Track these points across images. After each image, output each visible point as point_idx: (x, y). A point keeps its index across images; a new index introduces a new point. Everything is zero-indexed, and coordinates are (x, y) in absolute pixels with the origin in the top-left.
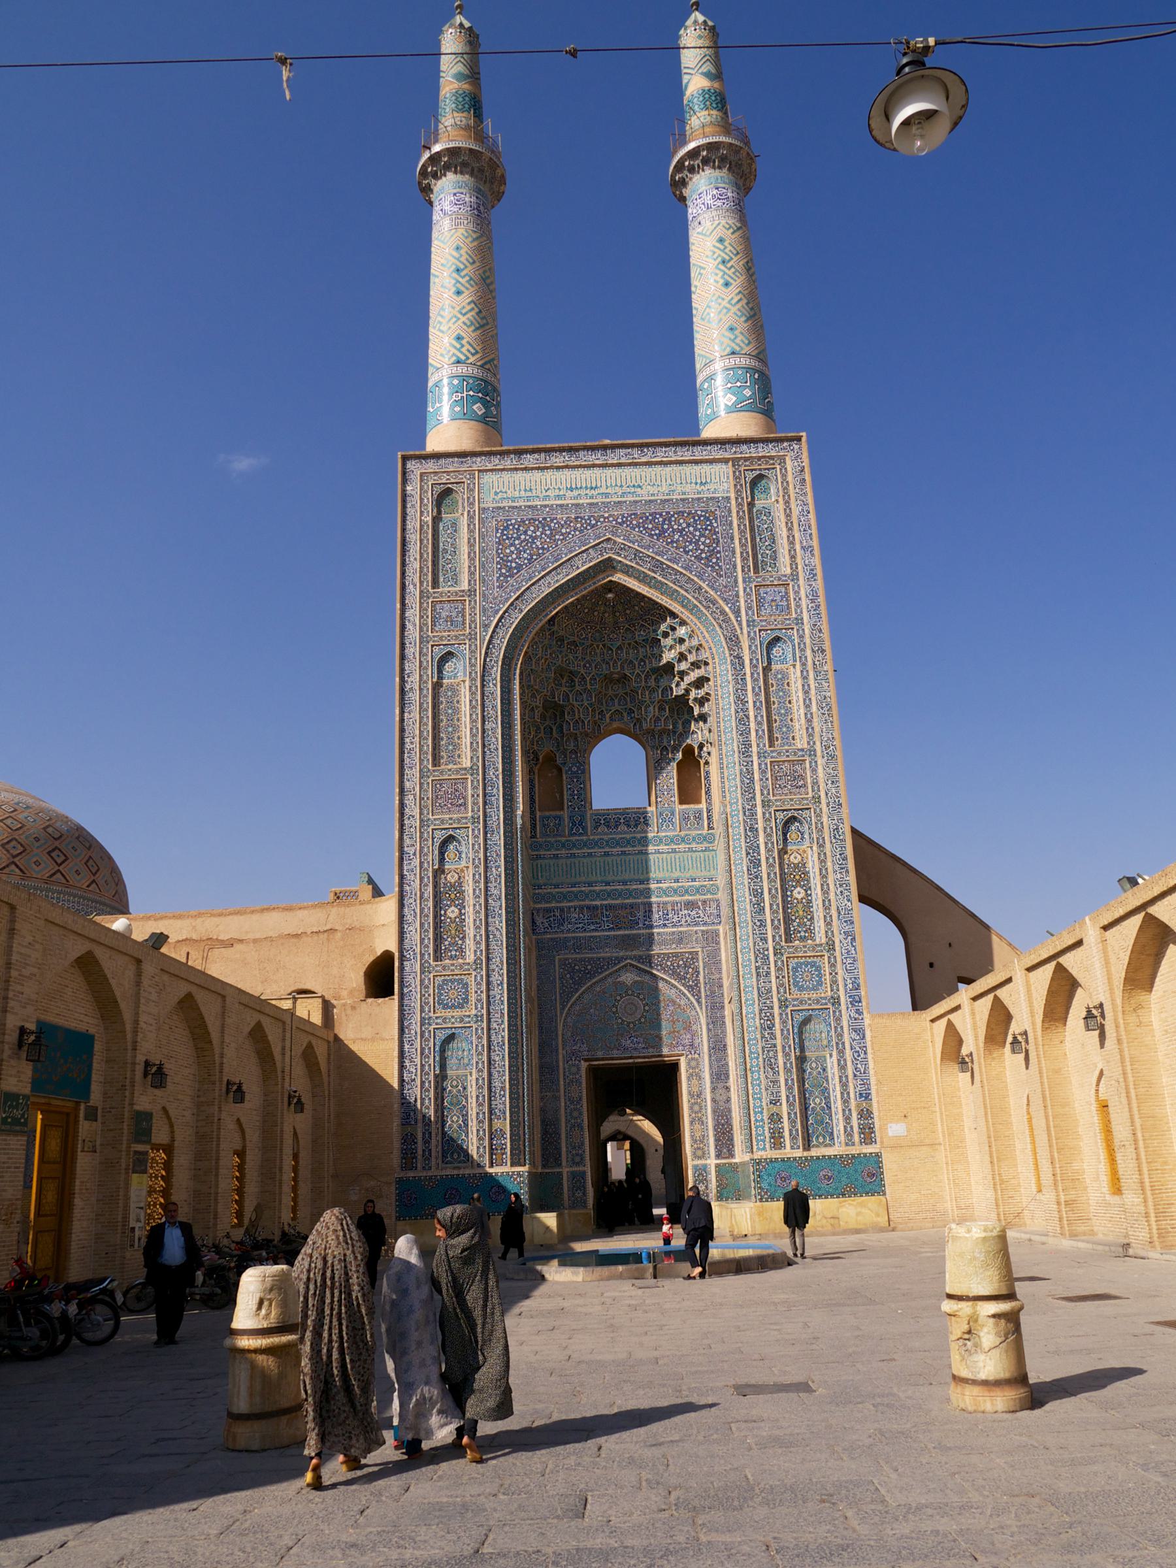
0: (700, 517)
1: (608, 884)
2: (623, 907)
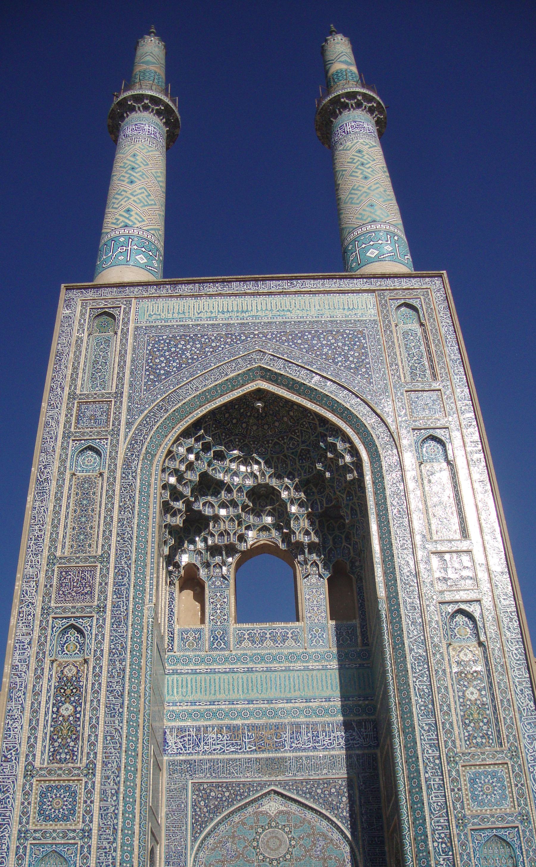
0: (348, 335)
1: (250, 702)
2: (266, 727)
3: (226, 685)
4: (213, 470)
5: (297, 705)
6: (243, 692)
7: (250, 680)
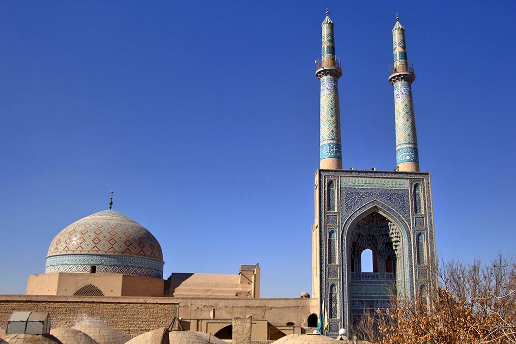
1: (366, 294)
2: (370, 301)
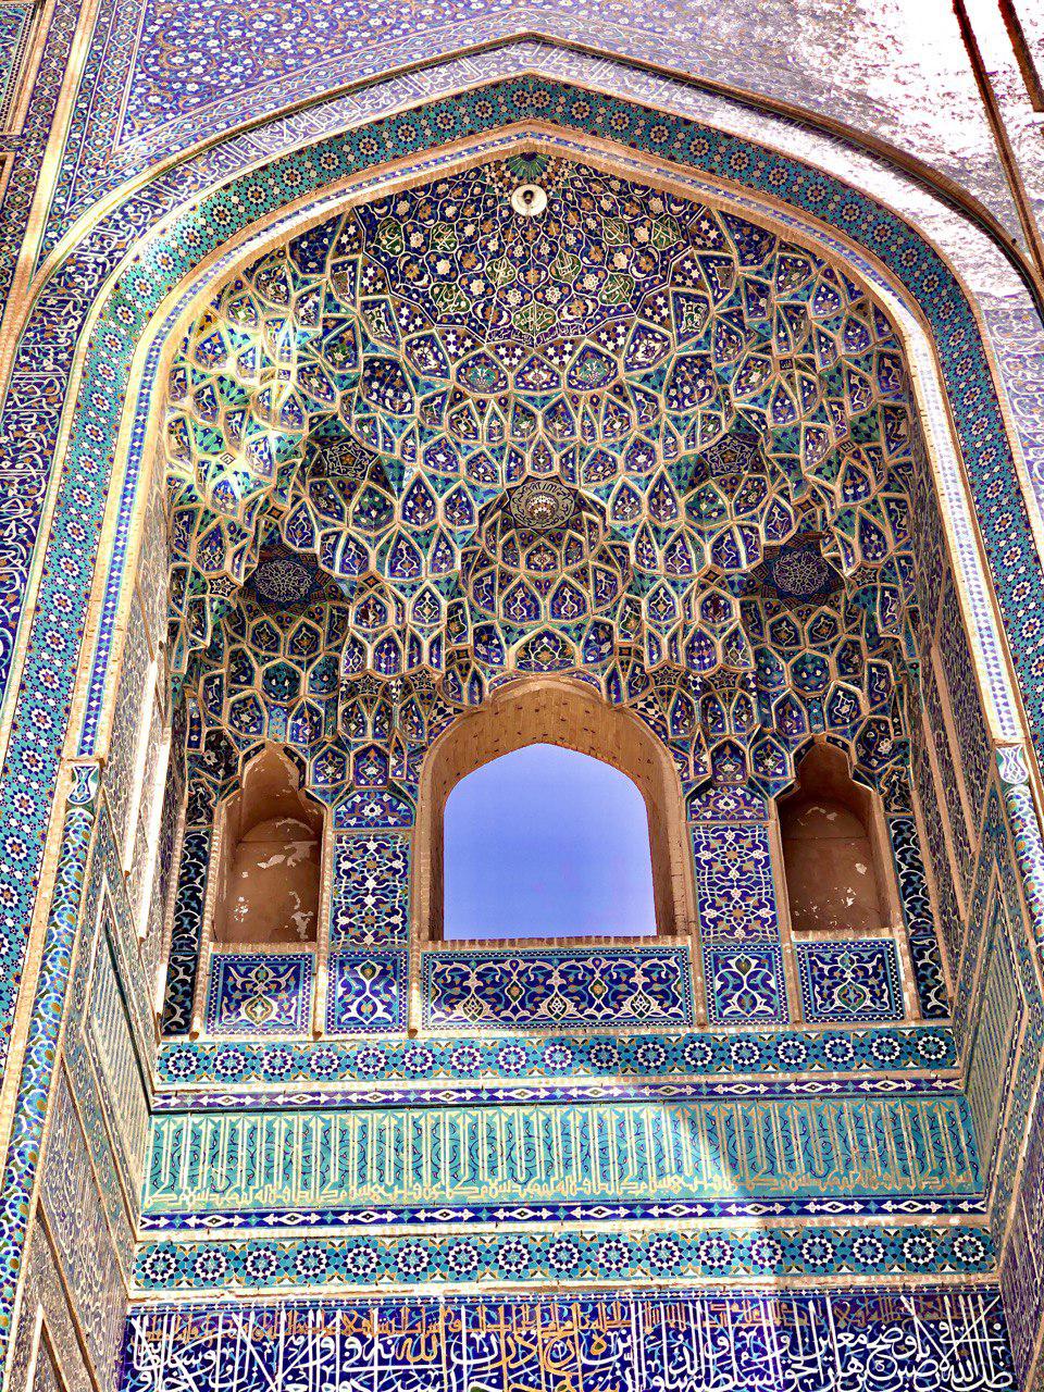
3: (390, 1154)
4: (361, 423)
5: (668, 1226)
6: (455, 1176)
7: (482, 1132)
